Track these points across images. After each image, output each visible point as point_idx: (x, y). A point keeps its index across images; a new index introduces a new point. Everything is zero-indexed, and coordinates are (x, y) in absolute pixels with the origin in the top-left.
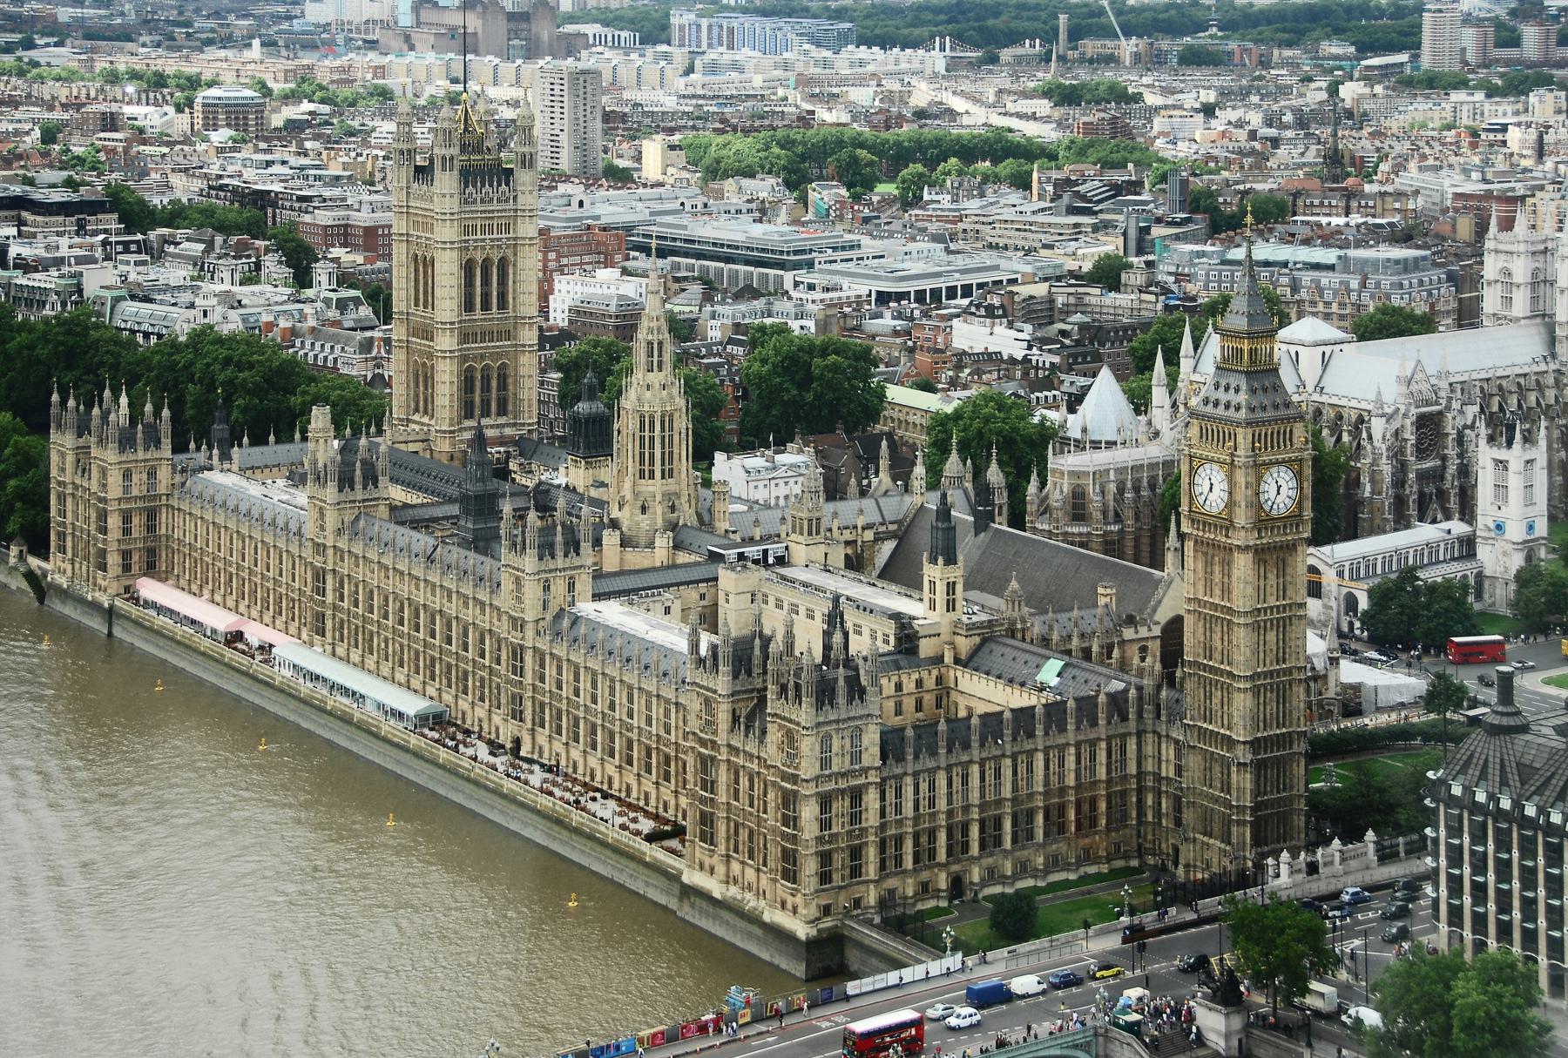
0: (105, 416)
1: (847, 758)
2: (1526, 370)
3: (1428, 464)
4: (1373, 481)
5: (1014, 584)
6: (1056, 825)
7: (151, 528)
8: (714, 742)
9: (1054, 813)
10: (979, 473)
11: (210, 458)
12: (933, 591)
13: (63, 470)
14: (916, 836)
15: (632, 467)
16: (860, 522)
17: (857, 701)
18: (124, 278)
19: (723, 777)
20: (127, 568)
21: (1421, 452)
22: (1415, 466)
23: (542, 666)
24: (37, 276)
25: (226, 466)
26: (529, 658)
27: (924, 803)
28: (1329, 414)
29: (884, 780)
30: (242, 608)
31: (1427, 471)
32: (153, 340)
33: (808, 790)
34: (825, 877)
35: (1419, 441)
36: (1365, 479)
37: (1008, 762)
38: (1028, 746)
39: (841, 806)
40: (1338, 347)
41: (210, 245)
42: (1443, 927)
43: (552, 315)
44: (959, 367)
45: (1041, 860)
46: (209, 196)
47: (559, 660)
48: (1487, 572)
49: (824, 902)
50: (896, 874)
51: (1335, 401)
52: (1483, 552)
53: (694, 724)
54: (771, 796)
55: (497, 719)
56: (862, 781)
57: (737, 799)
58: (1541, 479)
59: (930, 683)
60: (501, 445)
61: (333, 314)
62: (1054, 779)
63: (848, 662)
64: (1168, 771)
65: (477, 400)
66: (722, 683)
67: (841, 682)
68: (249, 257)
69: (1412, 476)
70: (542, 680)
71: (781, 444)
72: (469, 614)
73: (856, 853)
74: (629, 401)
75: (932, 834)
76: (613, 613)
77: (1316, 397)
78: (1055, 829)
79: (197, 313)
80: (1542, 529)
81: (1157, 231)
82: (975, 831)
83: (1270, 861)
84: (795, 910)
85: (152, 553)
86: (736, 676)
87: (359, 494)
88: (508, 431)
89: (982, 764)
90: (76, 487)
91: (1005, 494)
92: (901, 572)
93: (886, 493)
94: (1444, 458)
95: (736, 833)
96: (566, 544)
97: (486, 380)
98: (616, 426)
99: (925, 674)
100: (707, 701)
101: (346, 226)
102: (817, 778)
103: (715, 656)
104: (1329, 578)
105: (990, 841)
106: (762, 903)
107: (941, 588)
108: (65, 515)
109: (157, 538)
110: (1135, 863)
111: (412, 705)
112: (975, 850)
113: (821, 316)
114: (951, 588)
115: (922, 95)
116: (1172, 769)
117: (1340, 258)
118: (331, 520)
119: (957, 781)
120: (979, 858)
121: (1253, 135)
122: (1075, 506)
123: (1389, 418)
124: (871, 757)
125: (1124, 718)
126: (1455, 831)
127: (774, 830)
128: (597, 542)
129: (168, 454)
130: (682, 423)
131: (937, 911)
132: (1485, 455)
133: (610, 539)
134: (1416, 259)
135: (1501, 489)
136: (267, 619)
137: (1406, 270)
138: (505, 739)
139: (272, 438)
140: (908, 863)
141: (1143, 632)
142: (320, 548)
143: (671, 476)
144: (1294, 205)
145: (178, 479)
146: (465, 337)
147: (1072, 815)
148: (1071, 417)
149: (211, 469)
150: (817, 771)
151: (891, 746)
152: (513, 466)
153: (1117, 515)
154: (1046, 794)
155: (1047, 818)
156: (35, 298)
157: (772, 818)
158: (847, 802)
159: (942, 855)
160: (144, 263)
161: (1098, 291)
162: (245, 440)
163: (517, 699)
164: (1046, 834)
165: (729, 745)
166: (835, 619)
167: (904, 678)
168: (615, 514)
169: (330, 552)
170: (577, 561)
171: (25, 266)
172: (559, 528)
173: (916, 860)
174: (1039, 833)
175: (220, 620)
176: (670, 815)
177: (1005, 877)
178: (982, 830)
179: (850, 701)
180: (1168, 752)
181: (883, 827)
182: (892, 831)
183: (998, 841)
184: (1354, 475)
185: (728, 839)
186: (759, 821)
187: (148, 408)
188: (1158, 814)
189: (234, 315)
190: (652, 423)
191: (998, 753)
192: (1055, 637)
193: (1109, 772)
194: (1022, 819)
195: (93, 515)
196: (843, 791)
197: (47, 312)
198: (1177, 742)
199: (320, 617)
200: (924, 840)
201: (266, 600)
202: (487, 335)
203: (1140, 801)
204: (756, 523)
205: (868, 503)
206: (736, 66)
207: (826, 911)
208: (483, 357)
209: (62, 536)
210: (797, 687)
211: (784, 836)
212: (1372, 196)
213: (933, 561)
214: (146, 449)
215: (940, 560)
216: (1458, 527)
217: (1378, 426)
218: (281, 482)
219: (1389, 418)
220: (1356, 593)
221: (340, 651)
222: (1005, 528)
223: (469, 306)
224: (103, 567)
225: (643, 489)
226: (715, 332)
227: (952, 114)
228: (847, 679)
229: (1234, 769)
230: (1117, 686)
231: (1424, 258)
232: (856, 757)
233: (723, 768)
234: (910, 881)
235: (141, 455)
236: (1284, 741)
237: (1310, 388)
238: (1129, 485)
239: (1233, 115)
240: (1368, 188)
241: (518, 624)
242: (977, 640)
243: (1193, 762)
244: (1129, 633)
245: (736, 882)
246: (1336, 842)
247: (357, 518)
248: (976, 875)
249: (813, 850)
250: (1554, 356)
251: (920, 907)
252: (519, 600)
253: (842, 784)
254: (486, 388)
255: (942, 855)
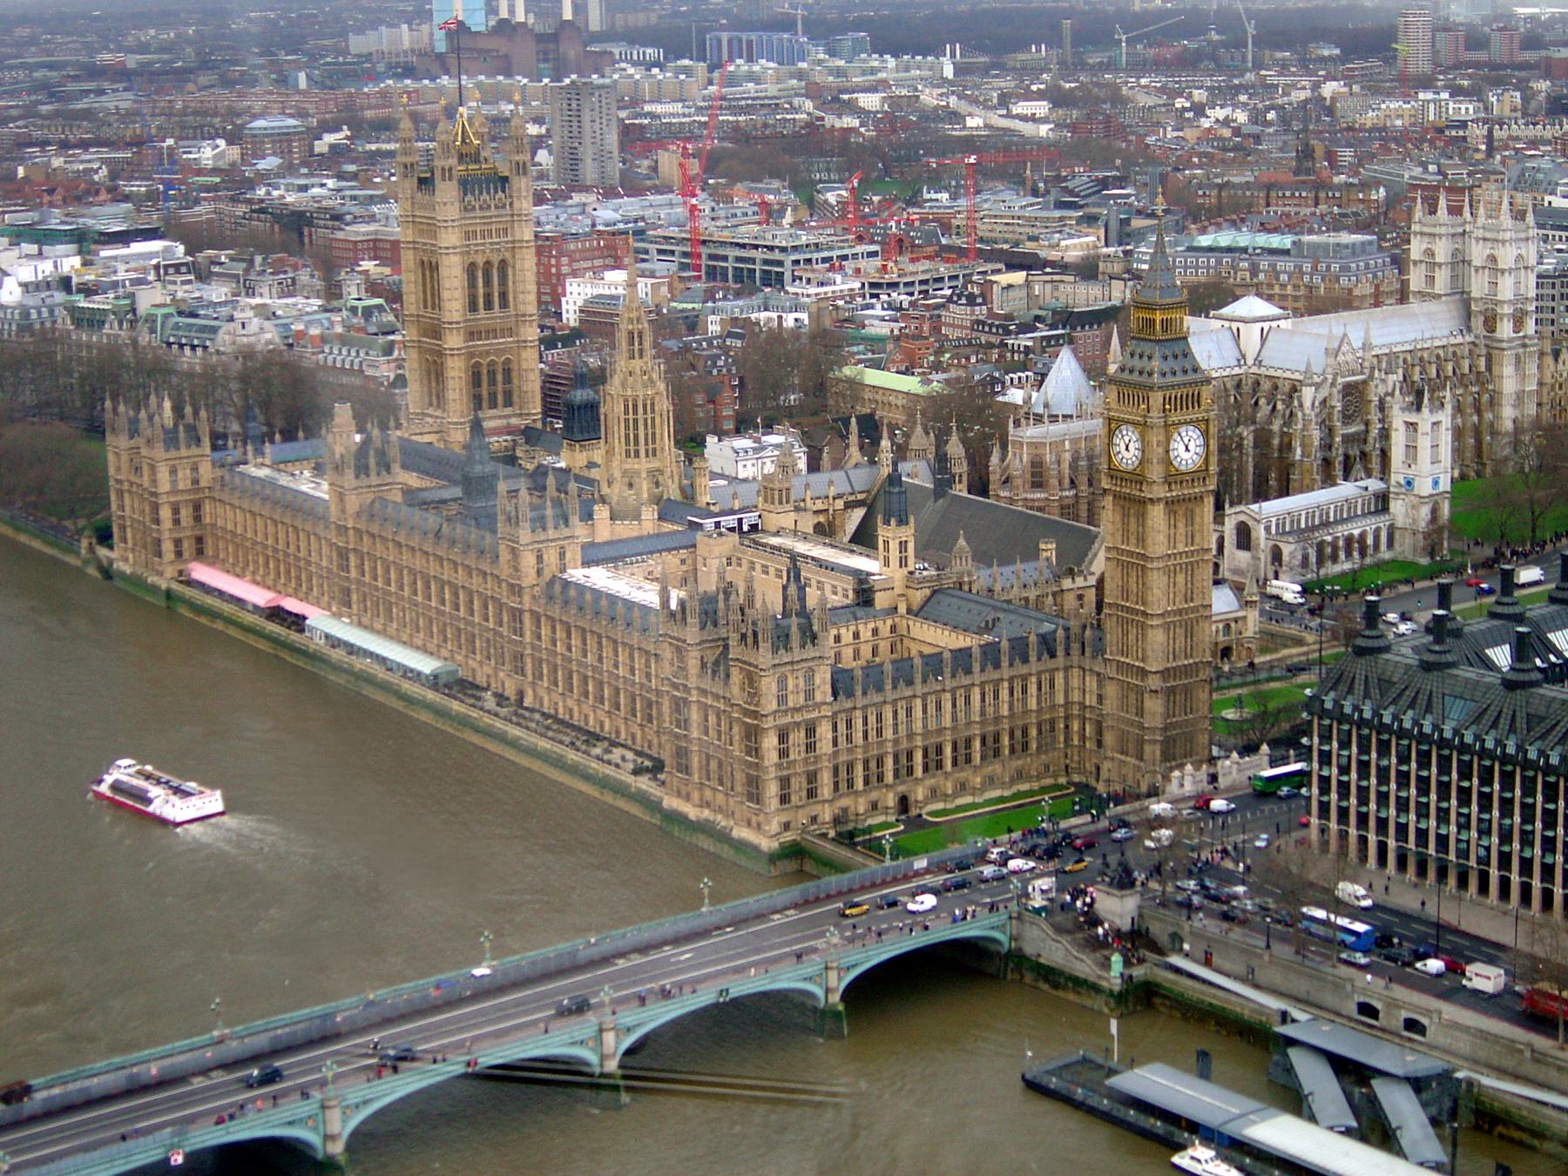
0: (151, 418)
1: (802, 695)
2: (1444, 342)
3: (1352, 429)
4: (1303, 445)
5: (962, 542)
6: (992, 748)
7: (198, 518)
8: (685, 686)
9: (990, 740)
10: (941, 443)
11: (245, 453)
12: (887, 549)
13: (118, 469)
14: (866, 763)
15: (619, 446)
16: (831, 495)
17: (809, 645)
18: (173, 295)
19: (695, 715)
20: (179, 554)
21: (1347, 418)
22: (1341, 430)
23: (538, 626)
24: (96, 298)
25: (260, 460)
26: (527, 616)
27: (872, 734)
28: (1266, 386)
29: (835, 714)
30: (280, 587)
31: (1352, 435)
32: (199, 351)
33: (769, 723)
34: (784, 799)
35: (1345, 408)
36: (1297, 444)
37: (948, 696)
38: (966, 681)
39: (798, 738)
40: (1274, 324)
41: (251, 262)
42: (1314, 821)
43: (564, 316)
44: (939, 352)
45: (978, 780)
46: (250, 219)
47: (553, 620)
48: (1399, 524)
49: (784, 818)
50: (848, 795)
51: (1272, 373)
52: (1396, 506)
53: (667, 670)
54: (736, 729)
55: (501, 675)
56: (815, 715)
57: (707, 734)
58: (1446, 438)
59: (885, 629)
60: (509, 434)
61: (358, 321)
62: (990, 710)
63: (803, 613)
64: (1090, 700)
65: (485, 393)
66: (692, 633)
67: (794, 629)
68: (285, 272)
69: (1338, 439)
70: (539, 638)
71: (769, 427)
72: (476, 582)
73: (812, 777)
74: (614, 386)
75: (880, 762)
76: (599, 578)
77: (1254, 370)
78: (991, 753)
79: (237, 325)
80: (1445, 485)
81: (1137, 223)
82: (918, 757)
83: (1176, 773)
84: (759, 826)
85: (199, 540)
86: (703, 627)
87: (374, 480)
88: (514, 421)
89: (924, 697)
90: (131, 484)
91: (965, 464)
92: (864, 539)
93: (856, 466)
94: (1367, 424)
95: (708, 764)
96: (556, 517)
97: (492, 374)
98: (602, 410)
99: (880, 624)
100: (678, 649)
101: (375, 241)
102: (775, 712)
103: (683, 610)
104: (1259, 534)
105: (932, 765)
106: (732, 823)
107: (894, 546)
108: (124, 509)
109: (204, 527)
110: (1062, 780)
111: (426, 665)
112: (919, 772)
113: (814, 308)
114: (903, 546)
115: (929, 98)
116: (1095, 698)
117: (1294, 243)
118: (353, 503)
119: (902, 714)
120: (922, 780)
121: (1237, 131)
122: (1033, 475)
123: (1318, 386)
124: (823, 692)
125: (1053, 655)
126: (1326, 737)
127: (741, 760)
128: (588, 516)
129: (208, 450)
130: (664, 405)
131: (886, 826)
132: (1398, 419)
133: (601, 513)
134: (1363, 244)
135: (1411, 449)
136: (301, 595)
137: (1354, 254)
138: (510, 691)
139: (301, 434)
140: (859, 784)
141: (1080, 582)
142: (343, 530)
143: (654, 455)
144: (1268, 196)
145: (219, 472)
146: (471, 335)
147: (1006, 741)
148: (1035, 395)
149: (246, 463)
150: (774, 706)
151: (841, 684)
152: (519, 453)
153: (1072, 482)
154: (982, 723)
155: (983, 743)
156: (93, 320)
157: (737, 750)
158: (803, 734)
159: (889, 777)
160: (189, 282)
161: (1071, 279)
162: (278, 437)
163: (519, 657)
164: (982, 758)
165: (698, 688)
166: (794, 573)
167: (861, 627)
168: (605, 490)
169: (351, 532)
170: (566, 532)
171: (88, 290)
172: (549, 503)
173: (866, 782)
174: (977, 758)
175: (259, 596)
176: (654, 753)
177: (946, 795)
178: (925, 755)
179: (803, 646)
180: (1091, 683)
181: (835, 754)
182: (843, 758)
183: (939, 765)
184: (1286, 440)
185: (701, 769)
186: (728, 753)
187: (188, 410)
188: (1083, 738)
189: (267, 324)
190: (635, 406)
191: (939, 688)
192: (998, 588)
193: (1039, 703)
194: (961, 746)
195: (147, 509)
196: (798, 724)
197: (106, 331)
198: (1098, 674)
199: (347, 592)
200: (873, 765)
201: (298, 578)
202: (491, 333)
203: (1067, 727)
204: (735, 496)
205: (839, 476)
206: (753, 78)
207: (786, 826)
208: (488, 353)
209: (123, 528)
210: (755, 634)
211: (750, 765)
212: (1340, 187)
213: (887, 522)
214: (188, 447)
215: (893, 522)
216: (1374, 485)
217: (1308, 394)
218: (307, 473)
219: (1318, 386)
220: (1281, 545)
221: (365, 620)
222: (965, 494)
223: (473, 307)
224: (159, 554)
225: (628, 466)
226: (714, 326)
227: (956, 117)
228: (800, 627)
229: (1146, 696)
230: (1047, 627)
231: (1370, 243)
232: (809, 694)
233: (694, 707)
234: (861, 800)
235: (184, 452)
236: (1187, 671)
237: (1250, 362)
238: (1083, 453)
239: (1220, 113)
240: (1336, 180)
241: (516, 590)
242: (928, 592)
243: (1111, 690)
244: (1067, 583)
245: (708, 805)
246: (1235, 755)
247: (373, 502)
248: (920, 793)
249: (772, 775)
250: (1469, 329)
251: (870, 822)
252: (516, 569)
253: (798, 718)
254: (492, 382)
255: (889, 777)
